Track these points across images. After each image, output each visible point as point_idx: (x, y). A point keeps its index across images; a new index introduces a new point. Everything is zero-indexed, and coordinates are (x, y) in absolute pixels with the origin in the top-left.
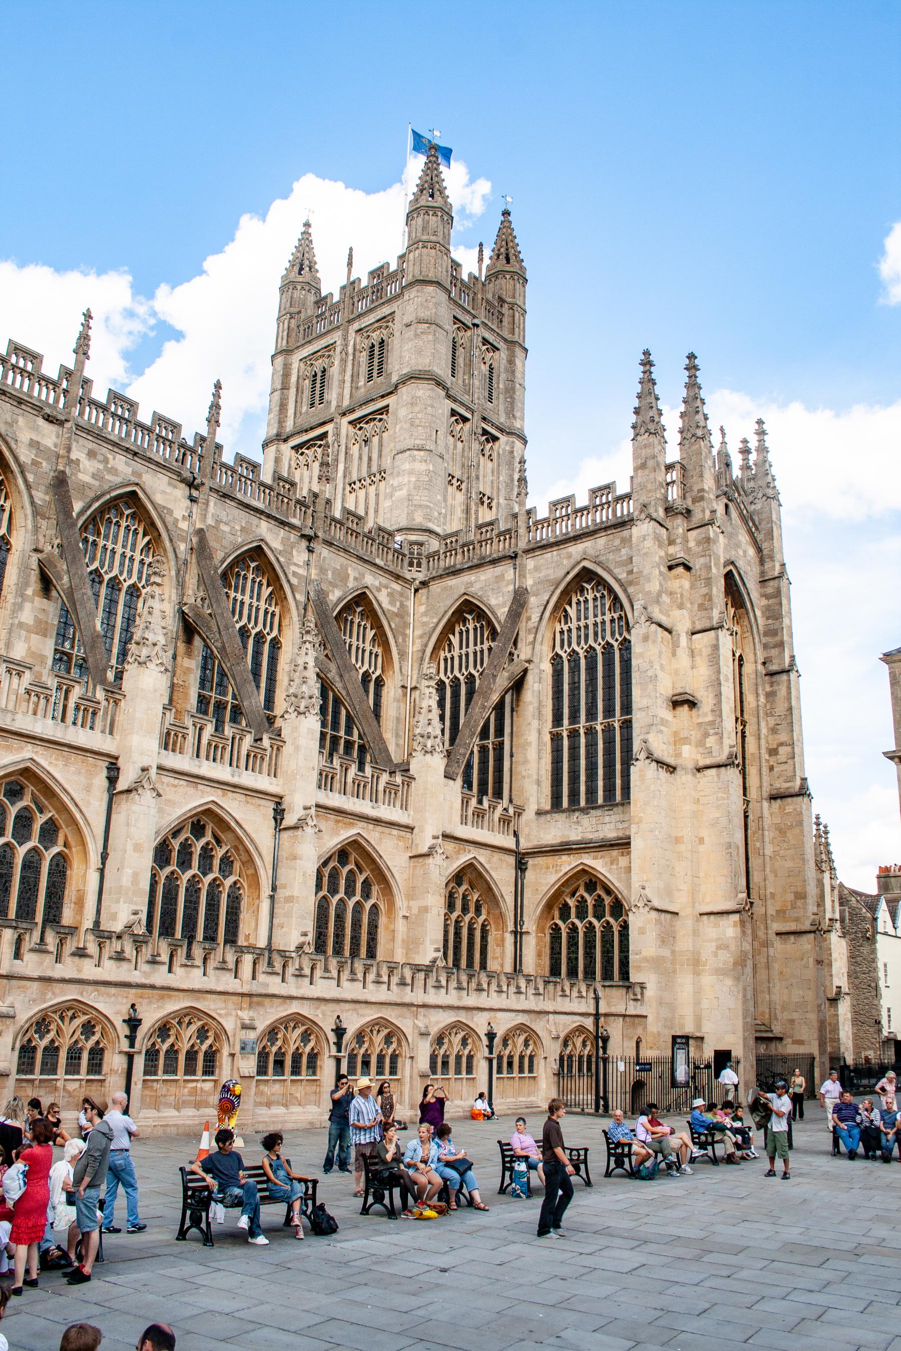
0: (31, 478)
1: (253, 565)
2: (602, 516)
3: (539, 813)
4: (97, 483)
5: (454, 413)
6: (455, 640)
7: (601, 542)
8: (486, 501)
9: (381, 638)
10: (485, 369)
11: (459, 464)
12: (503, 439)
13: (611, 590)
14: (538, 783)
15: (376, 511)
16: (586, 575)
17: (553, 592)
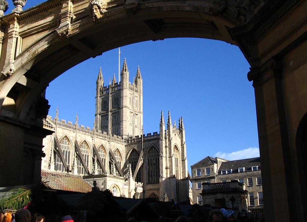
0: (72, 142)
1: (101, 147)
2: (155, 137)
3: (147, 184)
4: (80, 140)
5: (130, 112)
6: (132, 155)
7: (155, 141)
8: (136, 127)
9: (120, 155)
10: (135, 101)
11: (131, 121)
12: (139, 114)
13: (157, 150)
14: (146, 179)
15: (118, 131)
16: (153, 147)
17: (148, 149)
